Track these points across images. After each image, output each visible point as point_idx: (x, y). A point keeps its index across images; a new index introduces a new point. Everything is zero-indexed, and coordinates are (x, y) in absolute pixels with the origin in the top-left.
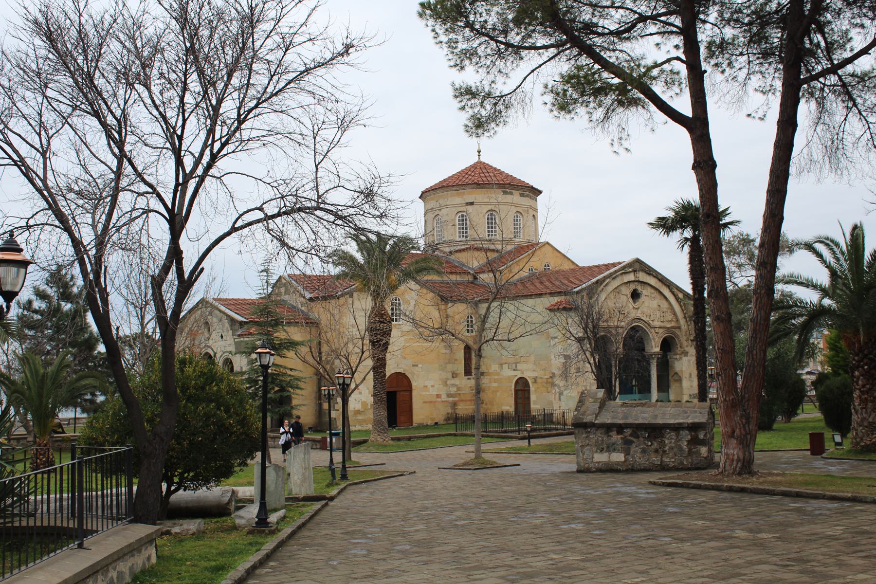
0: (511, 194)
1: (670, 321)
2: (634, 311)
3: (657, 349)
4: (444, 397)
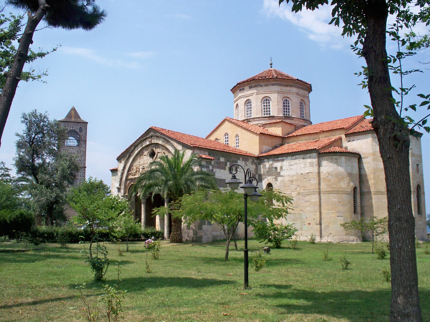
0: (243, 89)
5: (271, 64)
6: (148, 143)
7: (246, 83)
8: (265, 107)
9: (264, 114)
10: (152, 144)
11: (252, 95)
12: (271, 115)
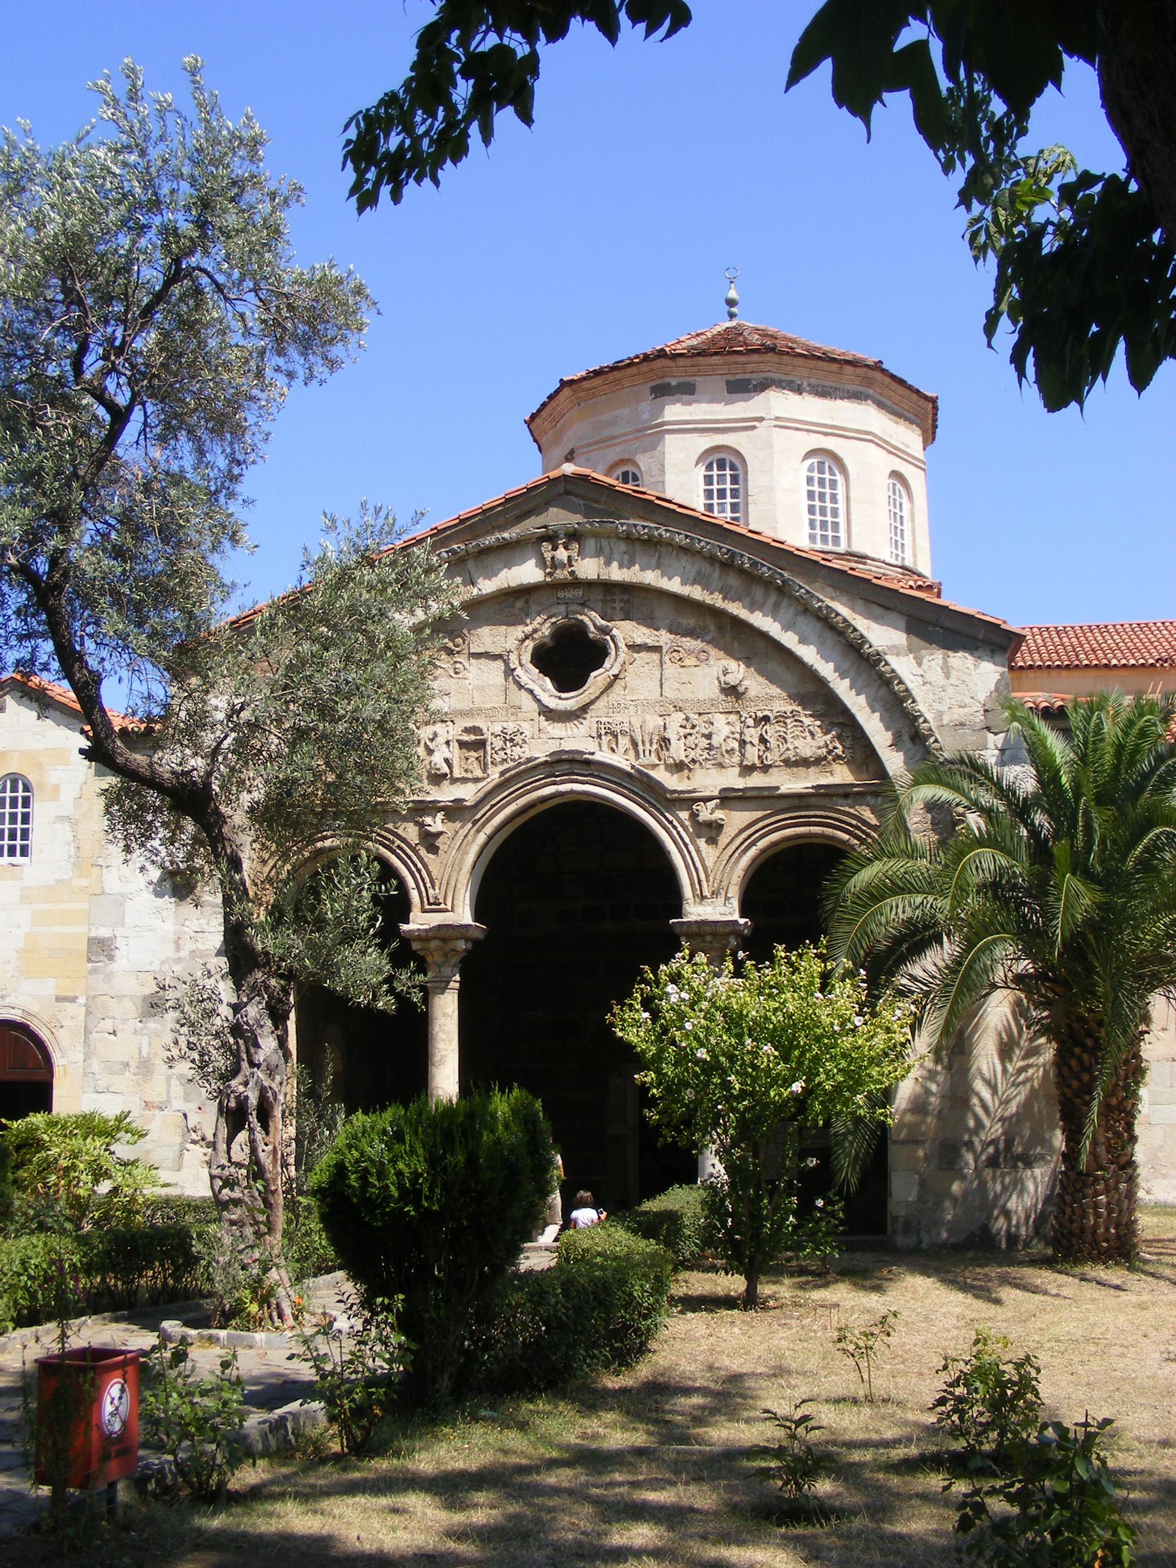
2: (557, 729)
6: (528, 572)
7: (715, 359)
8: (817, 503)
9: (812, 538)
10: (576, 583)
11: (749, 425)
12: (842, 548)
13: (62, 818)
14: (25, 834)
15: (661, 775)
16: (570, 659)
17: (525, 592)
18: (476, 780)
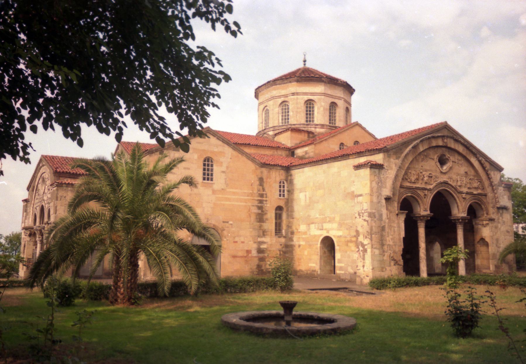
1: (476, 188)
2: (442, 176)
3: (464, 215)
4: (254, 253)
5: (305, 61)
6: (440, 143)
10: (446, 147)
11: (339, 98)
13: (223, 172)
14: (212, 175)
15: (458, 187)
16: (442, 161)
17: (438, 147)
18: (432, 184)
